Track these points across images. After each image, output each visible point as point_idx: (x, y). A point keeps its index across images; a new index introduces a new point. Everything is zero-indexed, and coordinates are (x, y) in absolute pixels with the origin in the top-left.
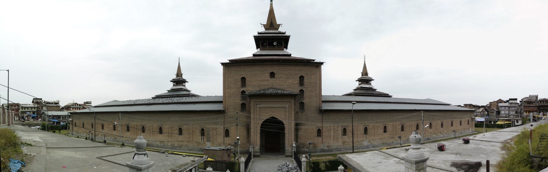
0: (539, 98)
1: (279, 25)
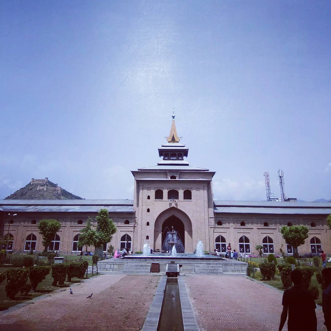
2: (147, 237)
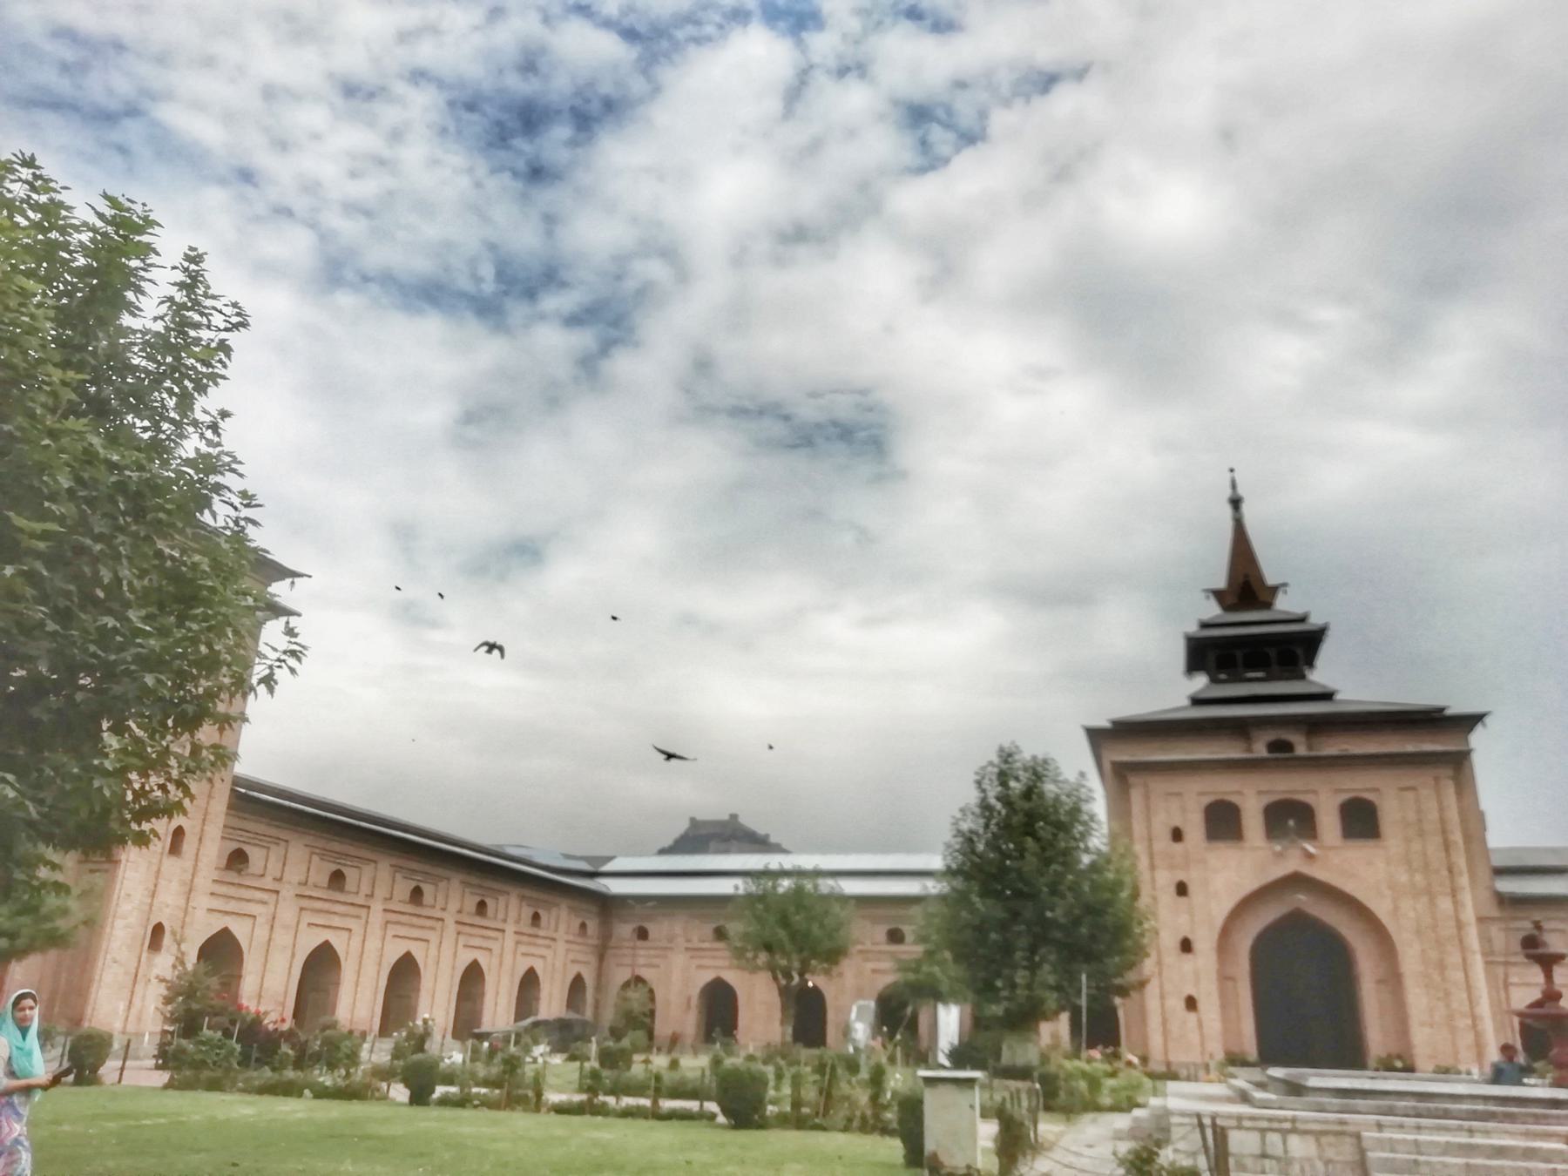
0: (1449, 712)
1: (1274, 590)
2: (1191, 1003)
